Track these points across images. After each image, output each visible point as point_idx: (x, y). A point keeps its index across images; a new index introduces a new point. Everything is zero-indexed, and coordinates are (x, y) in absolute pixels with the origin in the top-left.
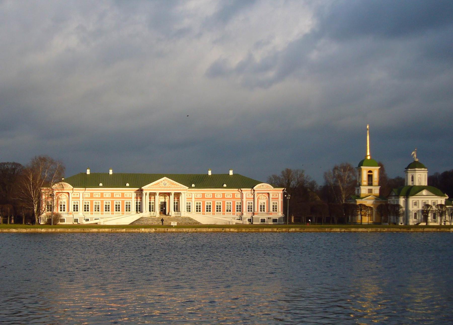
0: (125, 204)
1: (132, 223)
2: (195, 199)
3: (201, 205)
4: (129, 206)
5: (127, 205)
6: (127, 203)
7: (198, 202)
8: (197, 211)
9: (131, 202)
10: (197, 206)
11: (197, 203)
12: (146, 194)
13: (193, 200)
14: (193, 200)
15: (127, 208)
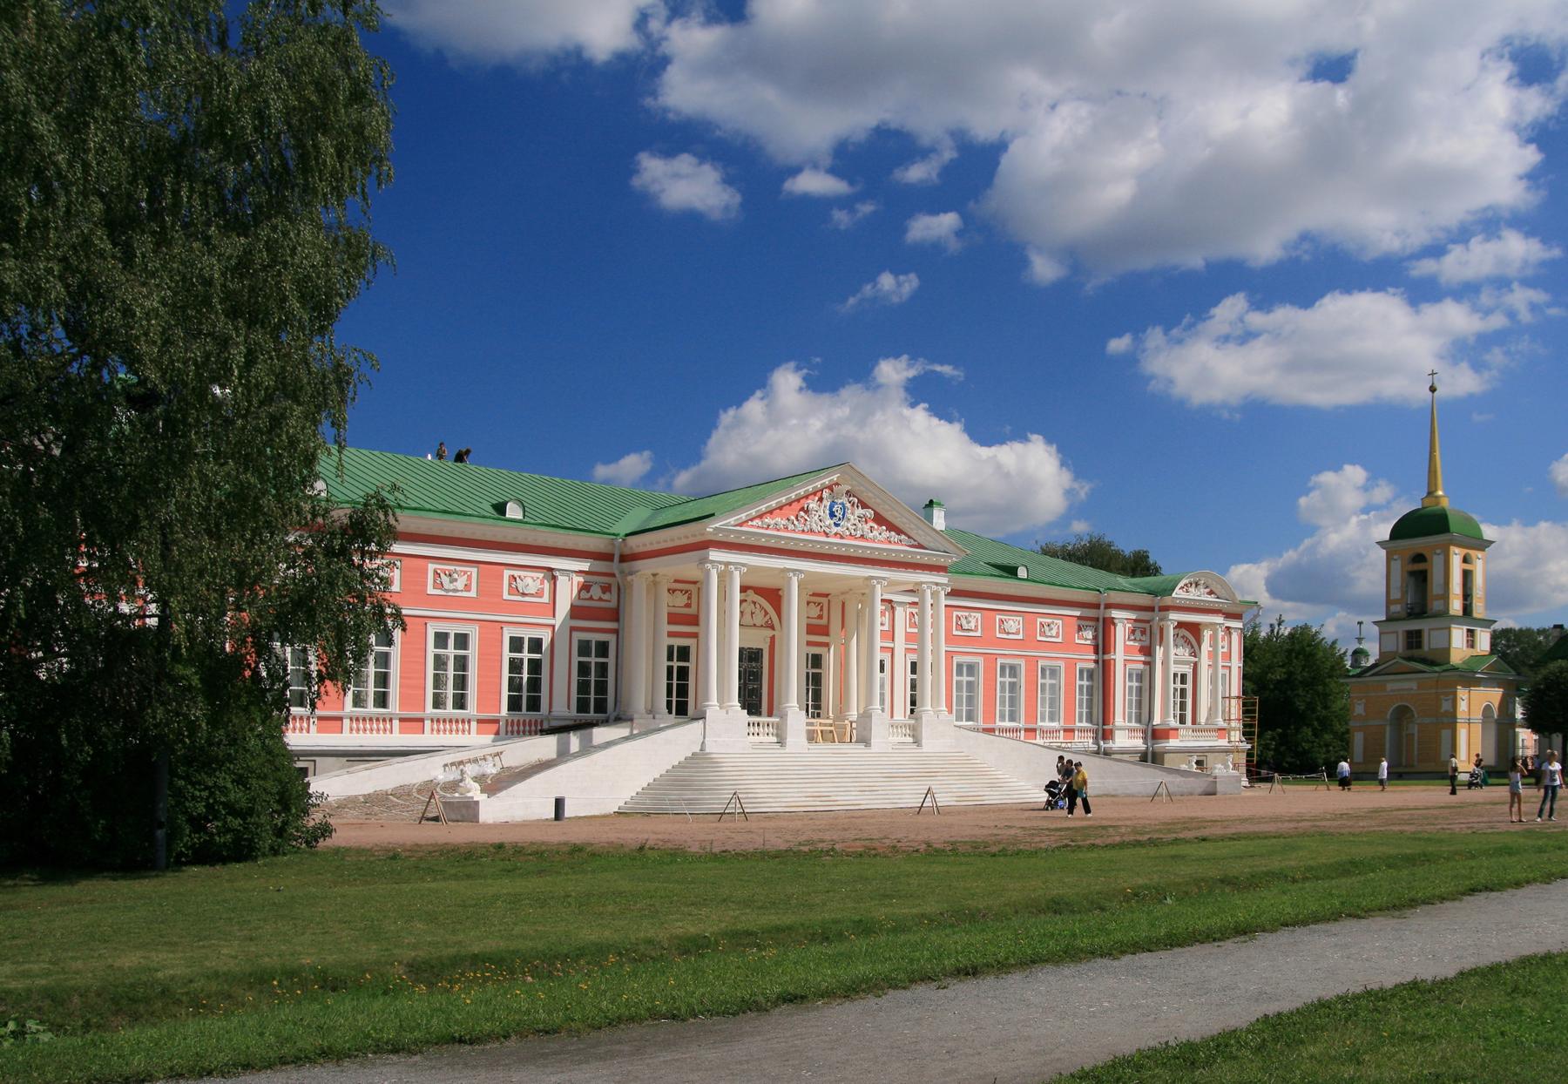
0: (507, 655)
6: (516, 644)
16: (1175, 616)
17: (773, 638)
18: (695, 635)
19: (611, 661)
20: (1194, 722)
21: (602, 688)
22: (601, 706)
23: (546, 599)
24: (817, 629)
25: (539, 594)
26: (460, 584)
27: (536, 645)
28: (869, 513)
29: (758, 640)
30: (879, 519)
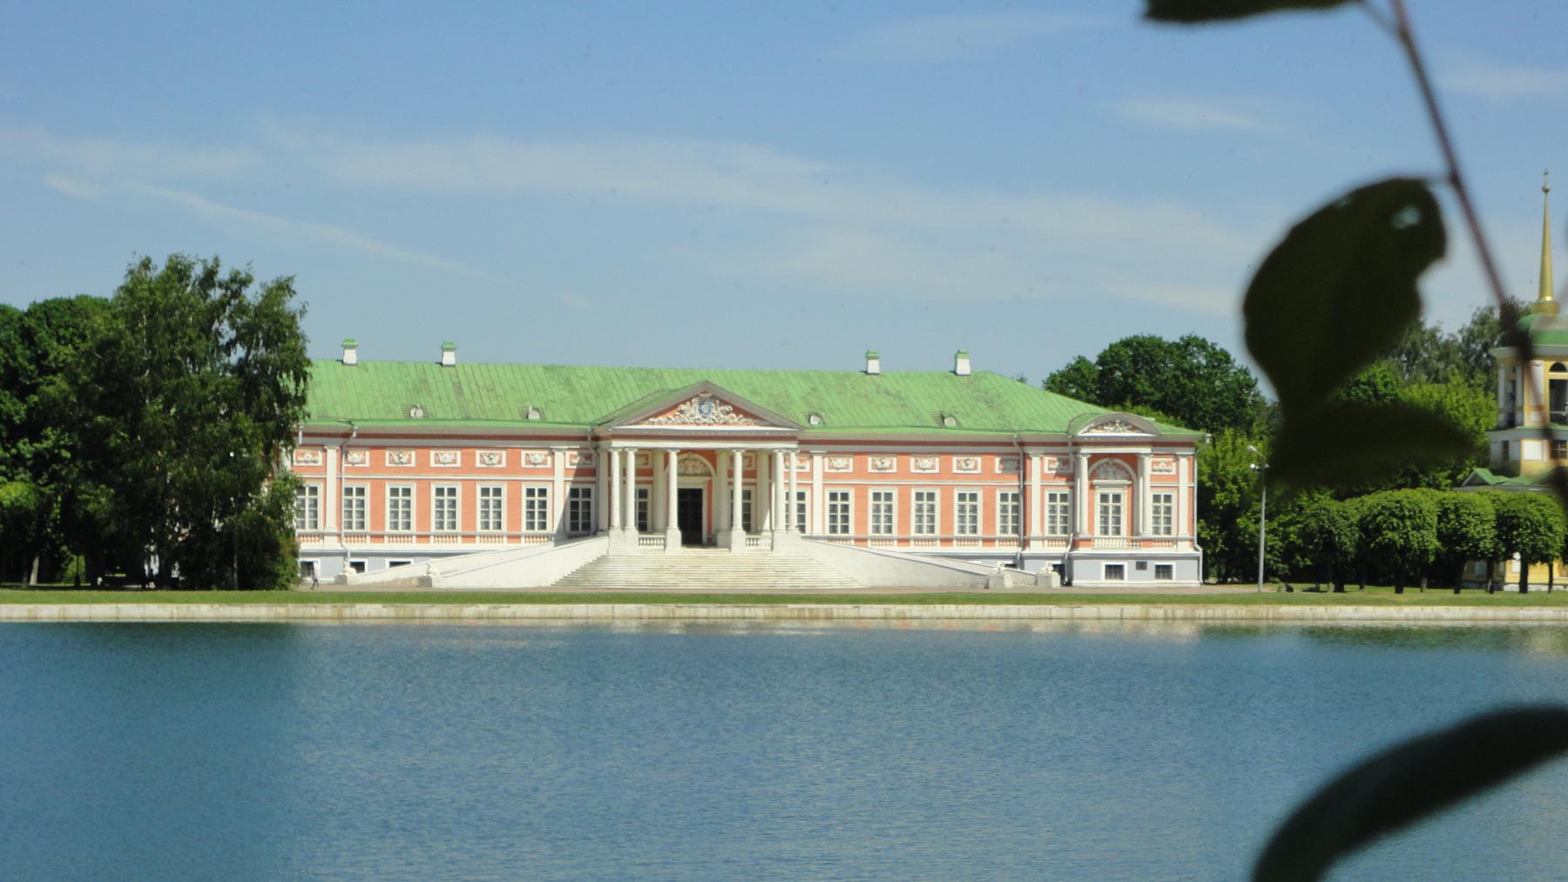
0: (525, 498)
1: (568, 581)
2: (826, 476)
3: (851, 502)
4: (543, 504)
5: (531, 504)
6: (530, 492)
7: (839, 491)
8: (833, 529)
9: (549, 488)
10: (833, 508)
11: (833, 496)
12: (624, 455)
13: (818, 481)
14: (818, 481)
15: (531, 515)
16: (1084, 450)
17: (710, 483)
18: (651, 482)
19: (592, 500)
20: (1134, 530)
21: (587, 515)
22: (587, 526)
23: (549, 465)
24: (749, 474)
25: (545, 462)
26: (495, 460)
27: (543, 492)
28: (727, 408)
29: (693, 483)
30: (737, 410)
